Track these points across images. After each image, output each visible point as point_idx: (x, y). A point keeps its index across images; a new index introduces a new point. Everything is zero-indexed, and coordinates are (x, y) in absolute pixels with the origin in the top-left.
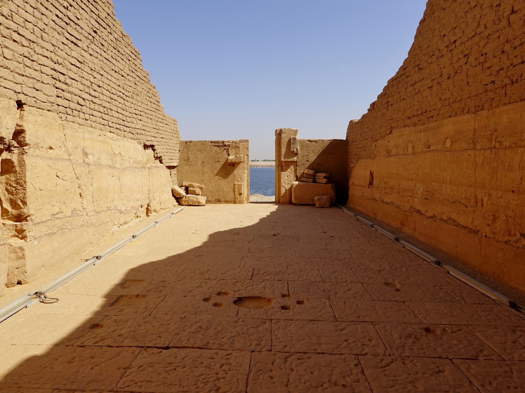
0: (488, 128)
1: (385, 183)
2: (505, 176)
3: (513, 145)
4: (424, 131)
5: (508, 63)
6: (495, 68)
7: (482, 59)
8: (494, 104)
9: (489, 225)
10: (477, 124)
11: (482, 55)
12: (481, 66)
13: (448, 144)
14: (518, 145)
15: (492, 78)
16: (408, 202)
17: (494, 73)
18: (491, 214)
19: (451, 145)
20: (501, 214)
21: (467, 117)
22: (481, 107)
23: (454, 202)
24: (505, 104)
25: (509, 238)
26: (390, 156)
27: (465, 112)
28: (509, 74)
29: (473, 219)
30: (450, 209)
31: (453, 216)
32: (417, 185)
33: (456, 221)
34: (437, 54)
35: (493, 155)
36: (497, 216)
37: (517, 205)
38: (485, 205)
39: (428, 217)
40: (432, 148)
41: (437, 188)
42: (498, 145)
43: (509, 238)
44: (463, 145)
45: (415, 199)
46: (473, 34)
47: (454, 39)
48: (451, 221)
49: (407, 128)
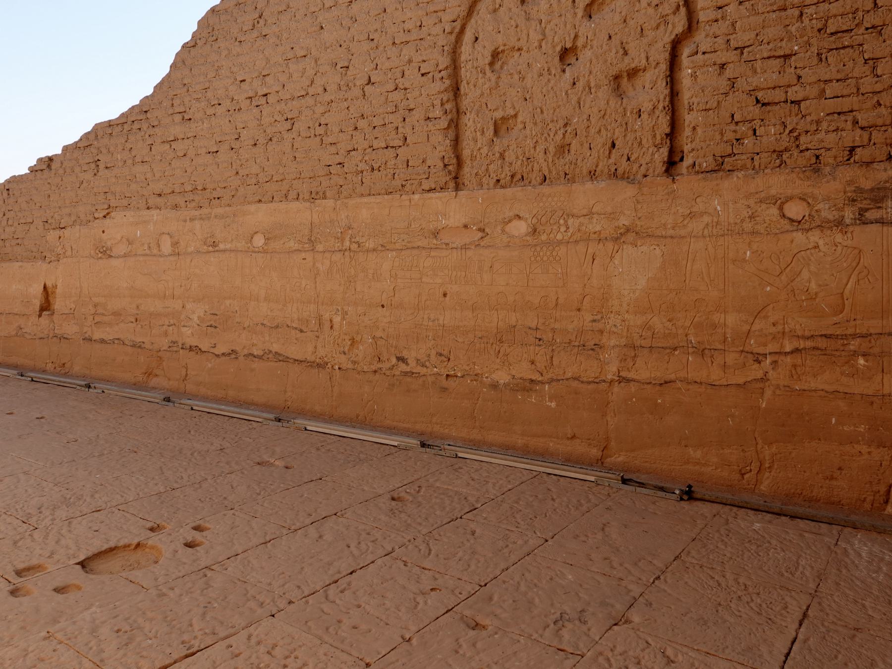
0: (336, 223)
1: (95, 306)
2: (370, 287)
3: (380, 248)
4: (201, 219)
5: (366, 144)
6: (343, 147)
7: (320, 130)
8: (345, 194)
9: (345, 353)
10: (315, 216)
11: (320, 125)
12: (318, 139)
13: (259, 241)
15: (338, 159)
16: (166, 334)
17: (342, 152)
18: (347, 337)
19: (266, 244)
20: (365, 336)
21: (295, 205)
22: (321, 194)
23: (277, 327)
25: (380, 365)
26: (111, 256)
27: (290, 197)
28: (366, 158)
29: (316, 347)
30: (267, 338)
31: (276, 348)
32: (189, 306)
33: (280, 355)
34: (227, 104)
35: (348, 260)
36: (358, 338)
37: (390, 322)
38: (336, 326)
39: (218, 356)
40: (222, 246)
41: (237, 308)
42: (354, 247)
43: (380, 365)
44: (292, 243)
45: (184, 329)
46: (303, 93)
47: (265, 91)
48: (270, 356)
49: (154, 212)
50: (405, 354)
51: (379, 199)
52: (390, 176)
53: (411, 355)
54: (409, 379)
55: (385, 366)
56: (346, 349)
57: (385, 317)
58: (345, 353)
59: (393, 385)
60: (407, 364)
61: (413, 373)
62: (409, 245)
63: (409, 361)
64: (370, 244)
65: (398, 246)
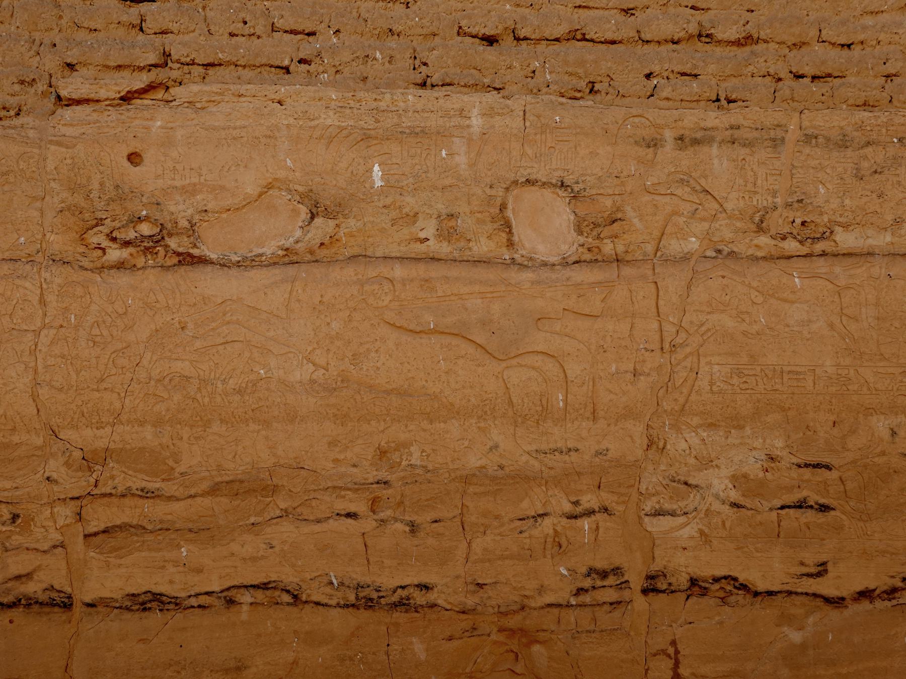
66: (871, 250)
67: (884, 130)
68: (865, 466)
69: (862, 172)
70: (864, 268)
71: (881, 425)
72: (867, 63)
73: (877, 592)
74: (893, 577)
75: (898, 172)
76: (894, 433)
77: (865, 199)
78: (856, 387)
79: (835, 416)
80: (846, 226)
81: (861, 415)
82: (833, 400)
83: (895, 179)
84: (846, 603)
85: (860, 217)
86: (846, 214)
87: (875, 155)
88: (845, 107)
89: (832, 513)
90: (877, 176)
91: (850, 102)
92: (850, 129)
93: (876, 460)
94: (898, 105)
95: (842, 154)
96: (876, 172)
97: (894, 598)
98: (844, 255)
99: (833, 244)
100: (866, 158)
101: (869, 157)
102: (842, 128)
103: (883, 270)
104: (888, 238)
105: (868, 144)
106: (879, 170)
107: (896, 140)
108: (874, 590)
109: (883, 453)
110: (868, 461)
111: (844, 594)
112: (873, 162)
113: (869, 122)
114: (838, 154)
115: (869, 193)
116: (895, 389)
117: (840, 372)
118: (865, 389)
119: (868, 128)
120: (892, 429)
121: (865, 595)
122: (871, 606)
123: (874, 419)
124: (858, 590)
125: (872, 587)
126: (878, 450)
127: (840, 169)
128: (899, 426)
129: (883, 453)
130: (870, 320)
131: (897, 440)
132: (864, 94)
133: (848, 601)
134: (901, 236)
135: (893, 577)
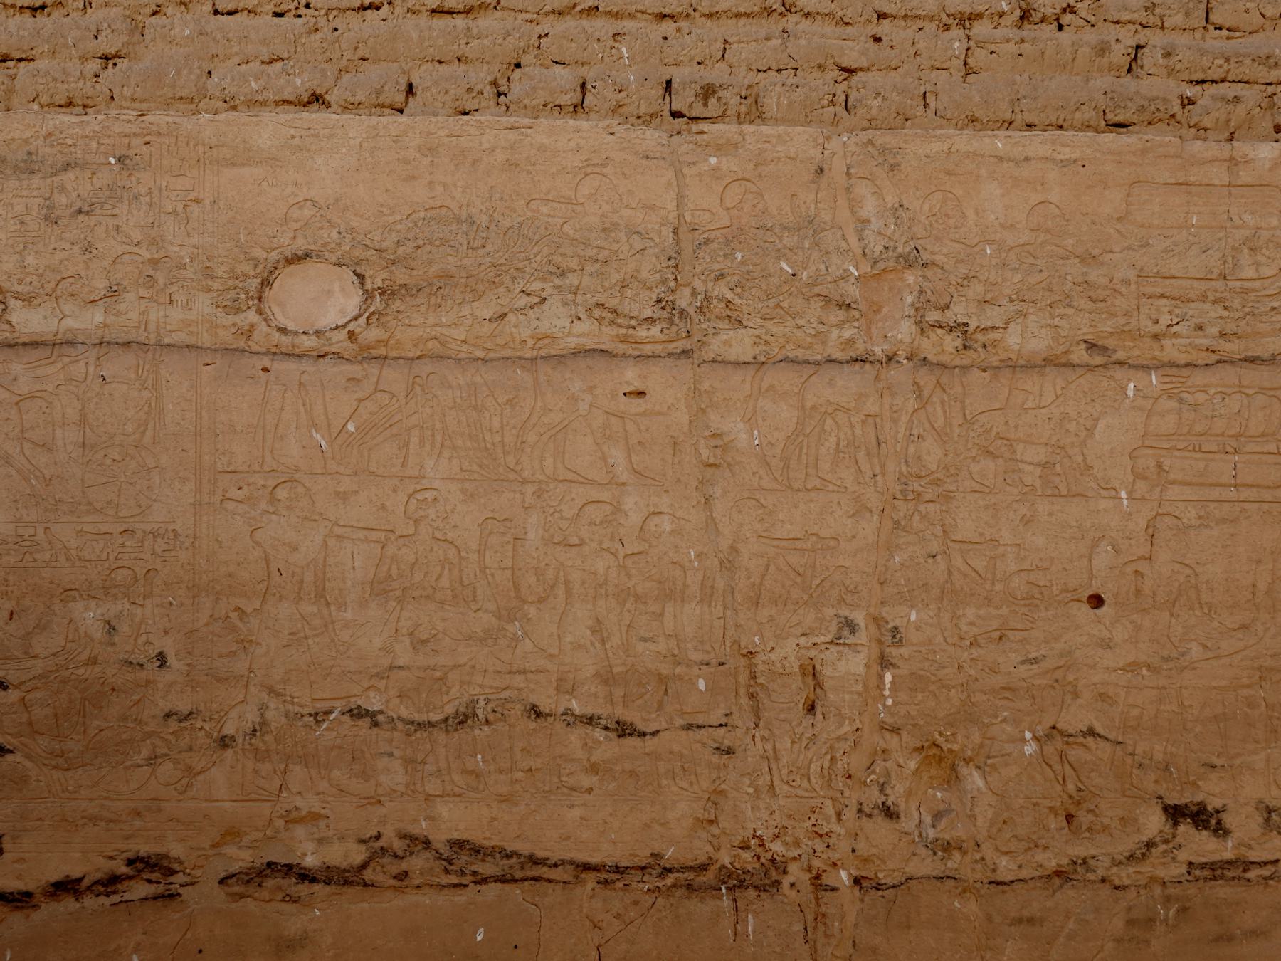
3: (1080, 355)
9: (890, 813)
14: (1120, 355)
24: (973, 120)
37: (1132, 668)
50: (1212, 792)
51: (1076, 144)
52: (1119, 55)
53: (1236, 796)
54: (1222, 891)
55: (1104, 850)
56: (896, 794)
57: (1107, 645)
58: (890, 813)
59: (1150, 921)
60: (1221, 831)
61: (1248, 865)
62: (1232, 348)
63: (1228, 819)
64: (1026, 338)
65: (1171, 350)
66: (70, 336)
67: (94, 145)
68: (65, 682)
69: (58, 212)
70: (59, 365)
71: (90, 616)
72: (65, 38)
73: (86, 882)
74: (111, 858)
75: (116, 211)
76: (111, 628)
77: (59, 256)
78: (47, 556)
79: (14, 603)
80: (27, 299)
81: (56, 601)
82: (11, 578)
83: (112, 222)
84: (35, 901)
85: (53, 284)
86: (28, 280)
87: (78, 185)
88: (36, 107)
89: (9, 757)
90: (81, 218)
91: (45, 99)
92: (40, 142)
93: (82, 671)
94: (125, 104)
95: (25, 183)
96: (80, 211)
97: (115, 892)
98: (25, 344)
99: (6, 327)
100: (62, 189)
101: (69, 188)
102: (26, 141)
103: (91, 369)
104: (99, 318)
105: (67, 167)
106: (85, 208)
107: (112, 160)
108: (80, 880)
109: (93, 661)
110: (67, 673)
111: (31, 886)
112: (74, 195)
113: (71, 131)
114: (17, 183)
115: (67, 246)
116: (111, 558)
117: (21, 531)
118: (62, 559)
119: (69, 142)
120: (109, 623)
121: (65, 887)
122: (78, 905)
123: (78, 606)
124: (53, 880)
125: (76, 874)
126: (85, 656)
127: (20, 208)
128: (119, 616)
129: (93, 661)
130: (70, 448)
131: (116, 639)
132: (65, 86)
133: (39, 898)
134: (119, 314)
135: (111, 858)
